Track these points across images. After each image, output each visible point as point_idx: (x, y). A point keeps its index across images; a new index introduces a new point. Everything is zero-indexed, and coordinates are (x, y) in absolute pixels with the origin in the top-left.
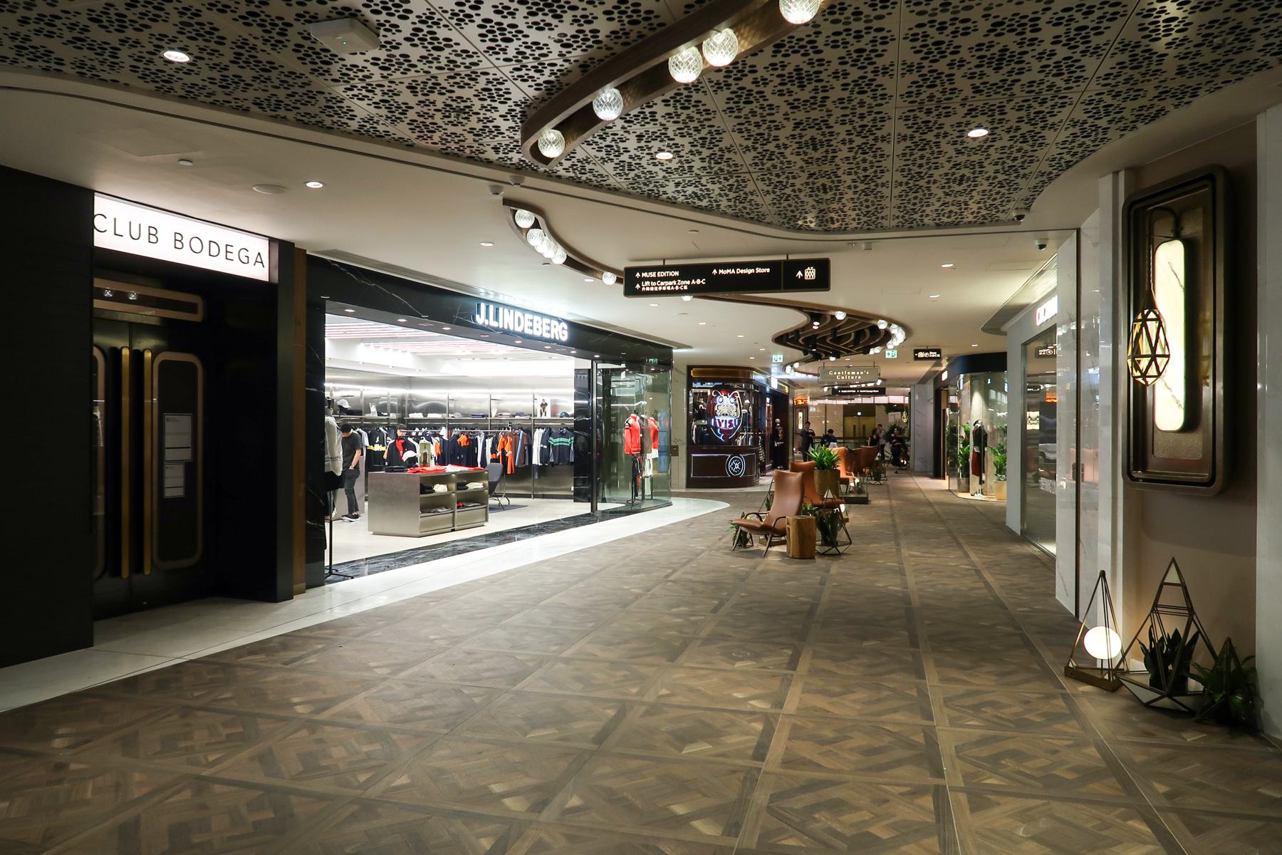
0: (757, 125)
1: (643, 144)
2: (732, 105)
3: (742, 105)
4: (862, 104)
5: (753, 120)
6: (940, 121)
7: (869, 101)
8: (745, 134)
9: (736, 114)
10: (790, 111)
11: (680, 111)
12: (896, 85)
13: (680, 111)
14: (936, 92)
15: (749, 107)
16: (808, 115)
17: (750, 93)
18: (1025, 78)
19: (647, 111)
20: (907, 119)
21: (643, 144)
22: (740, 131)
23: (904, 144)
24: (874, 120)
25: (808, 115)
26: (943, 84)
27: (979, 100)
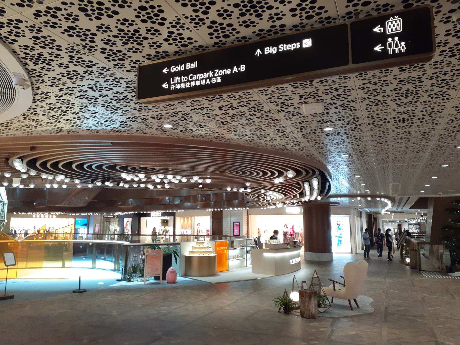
0: (300, 123)
1: (252, 132)
2: (286, 117)
3: (291, 117)
4: (346, 113)
5: (298, 121)
6: (384, 117)
7: (349, 112)
8: (296, 127)
9: (290, 120)
10: (313, 118)
11: (265, 121)
12: (361, 106)
13: (265, 121)
14: (380, 107)
15: (294, 117)
16: (322, 118)
17: (293, 113)
18: (421, 100)
19: (251, 121)
20: (369, 117)
21: (252, 132)
22: (293, 126)
23: (370, 126)
24: (353, 119)
25: (322, 118)
26: (382, 104)
27: (401, 109)
